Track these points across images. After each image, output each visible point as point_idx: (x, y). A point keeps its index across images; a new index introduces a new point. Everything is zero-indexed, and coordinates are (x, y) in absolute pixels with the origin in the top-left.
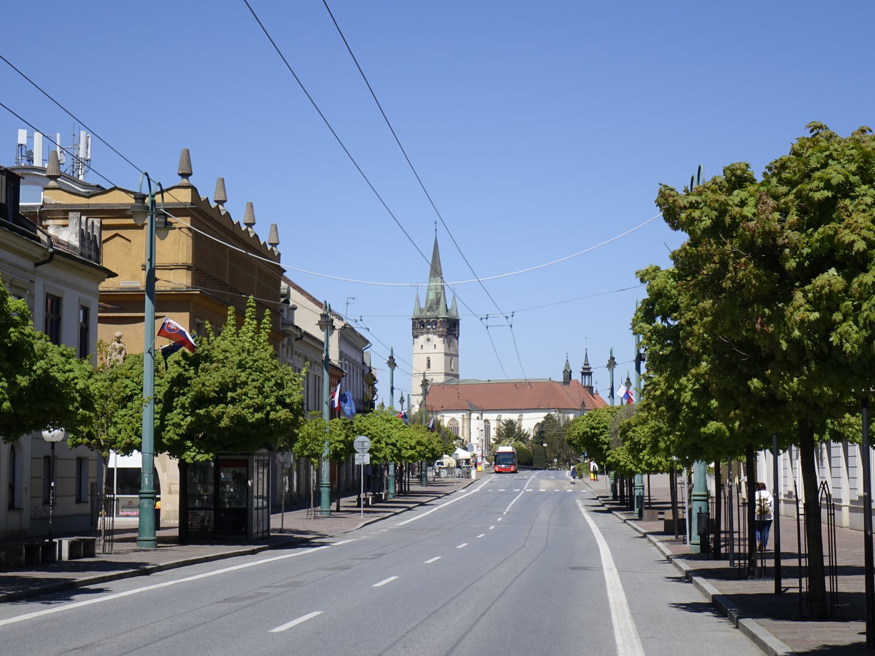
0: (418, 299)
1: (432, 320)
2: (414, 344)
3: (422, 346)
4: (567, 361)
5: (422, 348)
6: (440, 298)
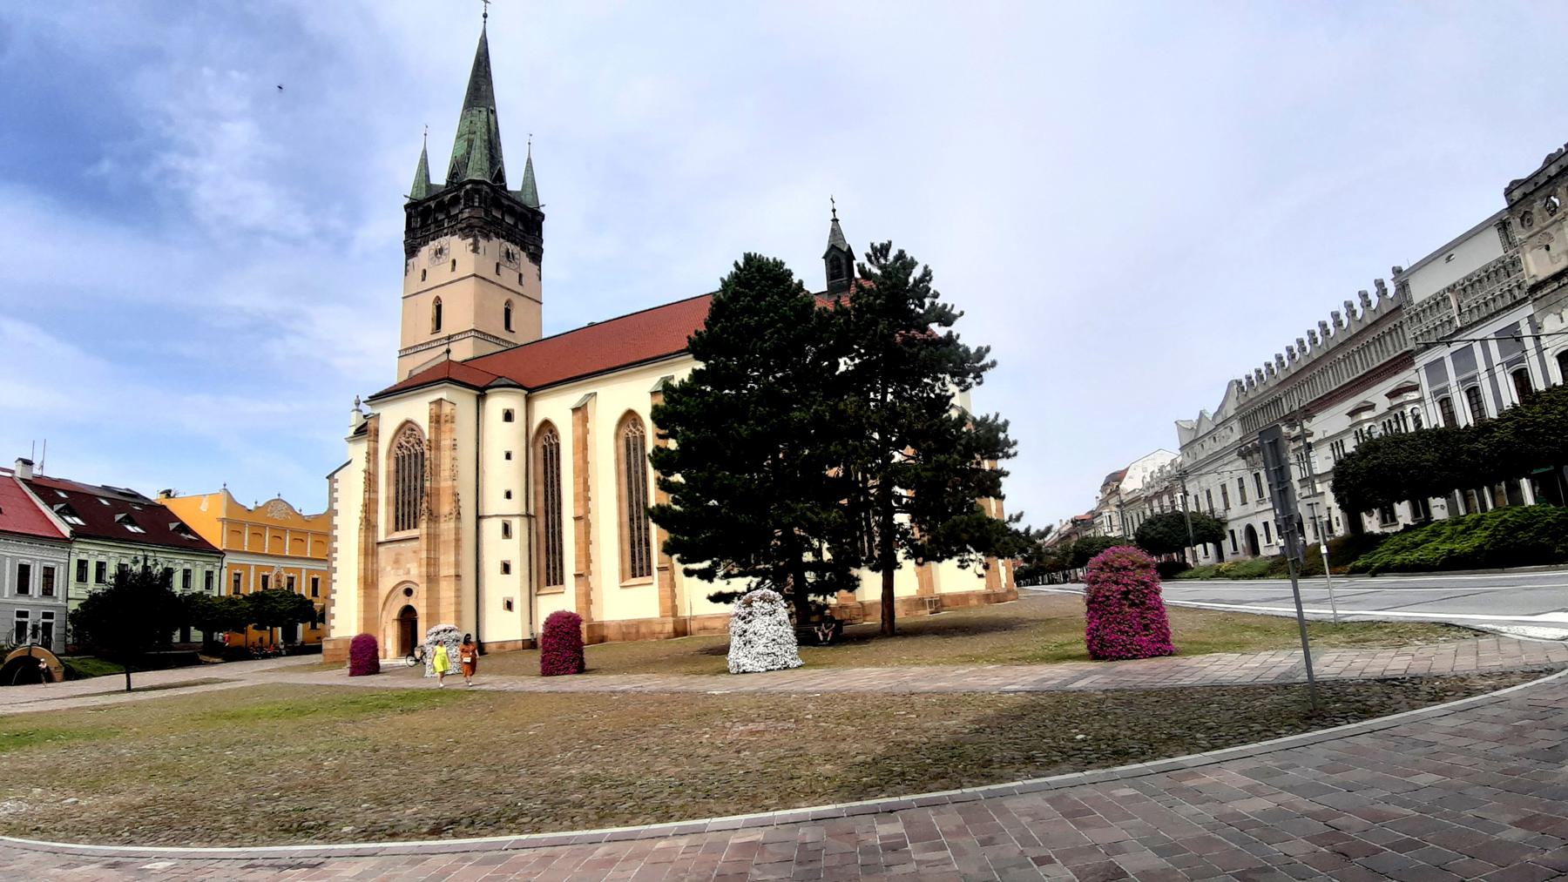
0: (424, 163)
1: (449, 196)
2: (406, 271)
3: (425, 272)
4: (835, 220)
5: (423, 279)
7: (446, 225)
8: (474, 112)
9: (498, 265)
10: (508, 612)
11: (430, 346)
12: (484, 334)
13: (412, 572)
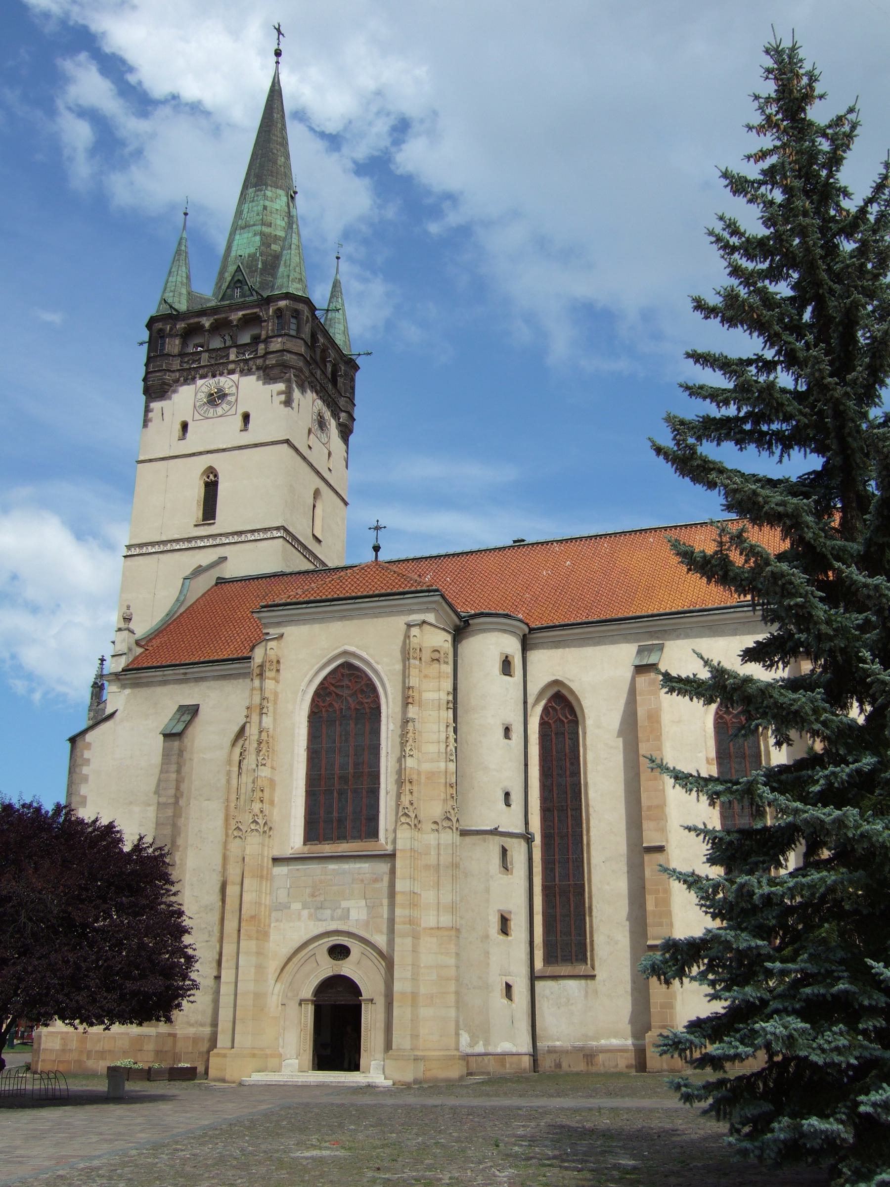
2: (146, 423)
3: (185, 426)
6: (277, 257)
7: (232, 357)
8: (269, 193)
9: (310, 431)
10: (505, 1001)
11: (193, 544)
12: (294, 538)
13: (354, 915)
